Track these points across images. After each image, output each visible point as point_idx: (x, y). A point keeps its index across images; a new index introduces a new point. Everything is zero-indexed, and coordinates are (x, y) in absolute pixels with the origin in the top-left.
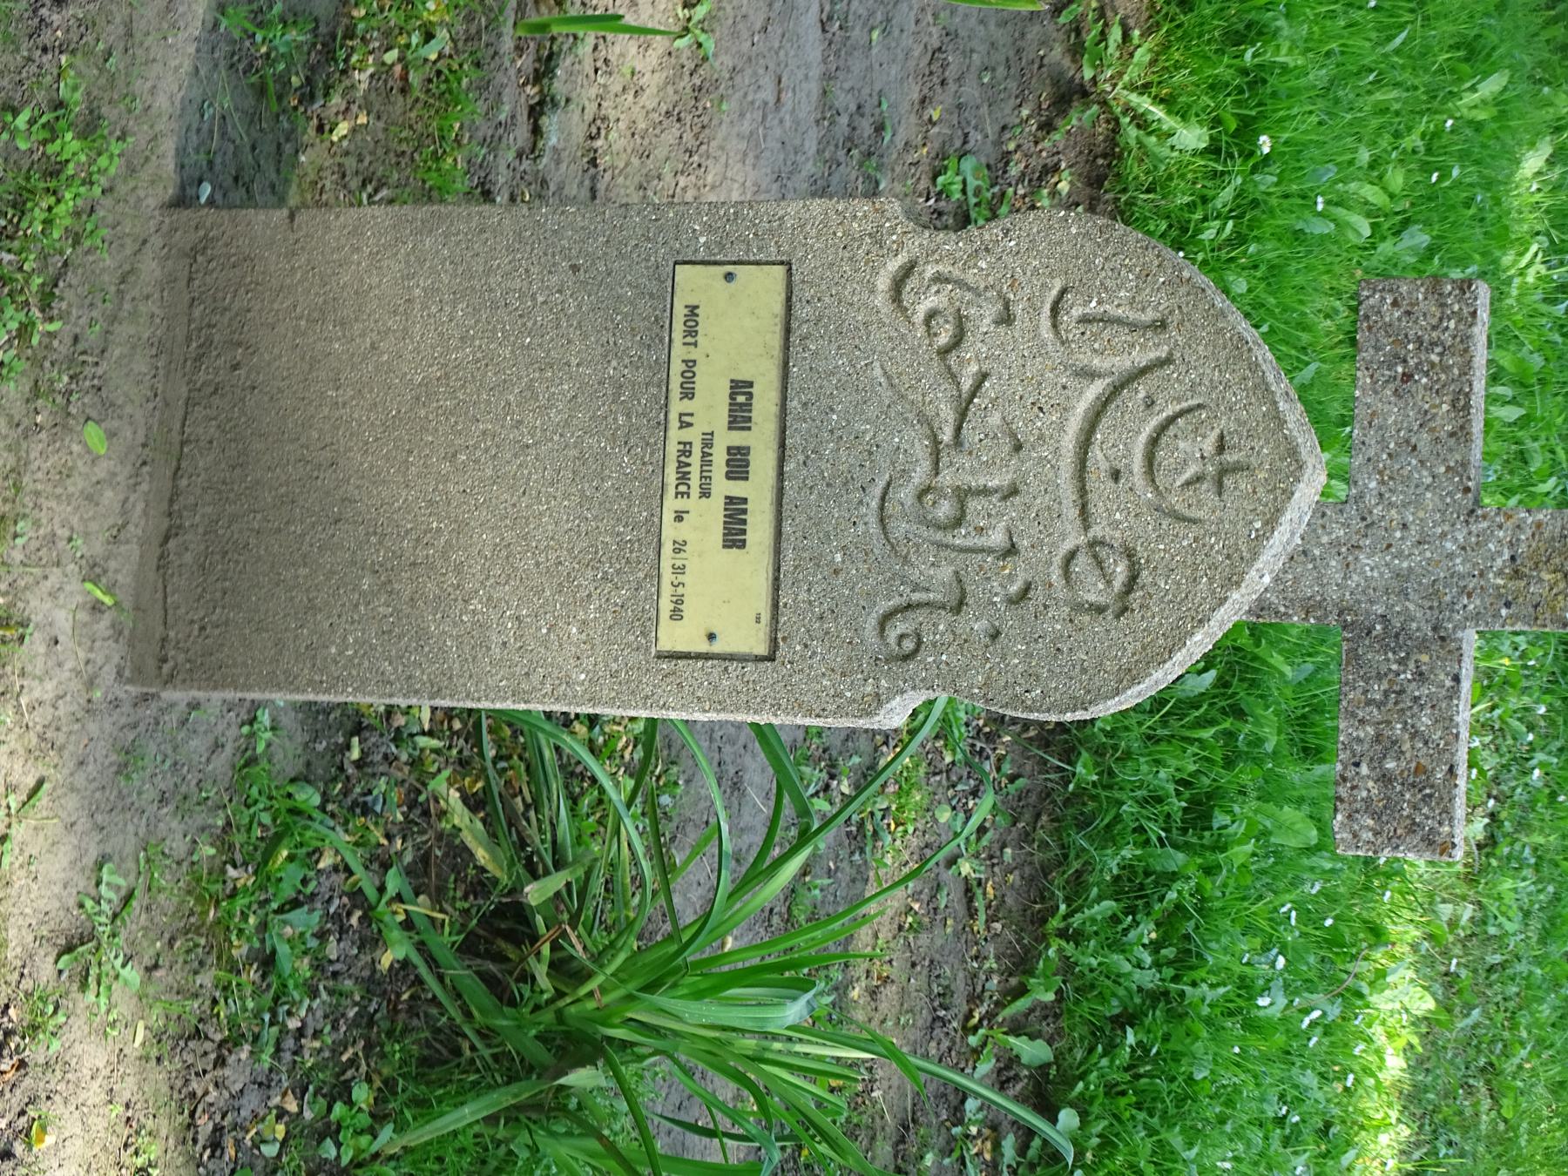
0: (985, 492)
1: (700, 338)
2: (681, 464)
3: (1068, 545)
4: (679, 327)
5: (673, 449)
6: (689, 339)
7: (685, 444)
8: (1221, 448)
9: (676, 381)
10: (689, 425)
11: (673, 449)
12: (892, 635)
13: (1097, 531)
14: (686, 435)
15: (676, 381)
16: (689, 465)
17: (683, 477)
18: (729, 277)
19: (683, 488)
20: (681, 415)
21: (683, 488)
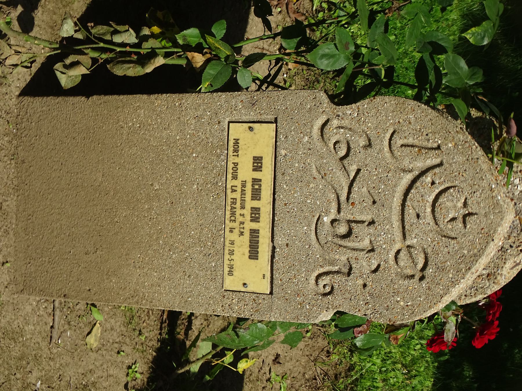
0: (363, 222)
1: (240, 153)
2: (232, 208)
3: (397, 246)
4: (231, 149)
5: (229, 201)
6: (235, 154)
7: (234, 199)
8: (465, 204)
9: (230, 171)
10: (236, 191)
11: (229, 201)
12: (321, 286)
13: (410, 241)
14: (234, 195)
15: (230, 171)
16: (236, 208)
17: (233, 214)
18: (251, 129)
19: (233, 218)
20: (232, 186)
21: (233, 218)
